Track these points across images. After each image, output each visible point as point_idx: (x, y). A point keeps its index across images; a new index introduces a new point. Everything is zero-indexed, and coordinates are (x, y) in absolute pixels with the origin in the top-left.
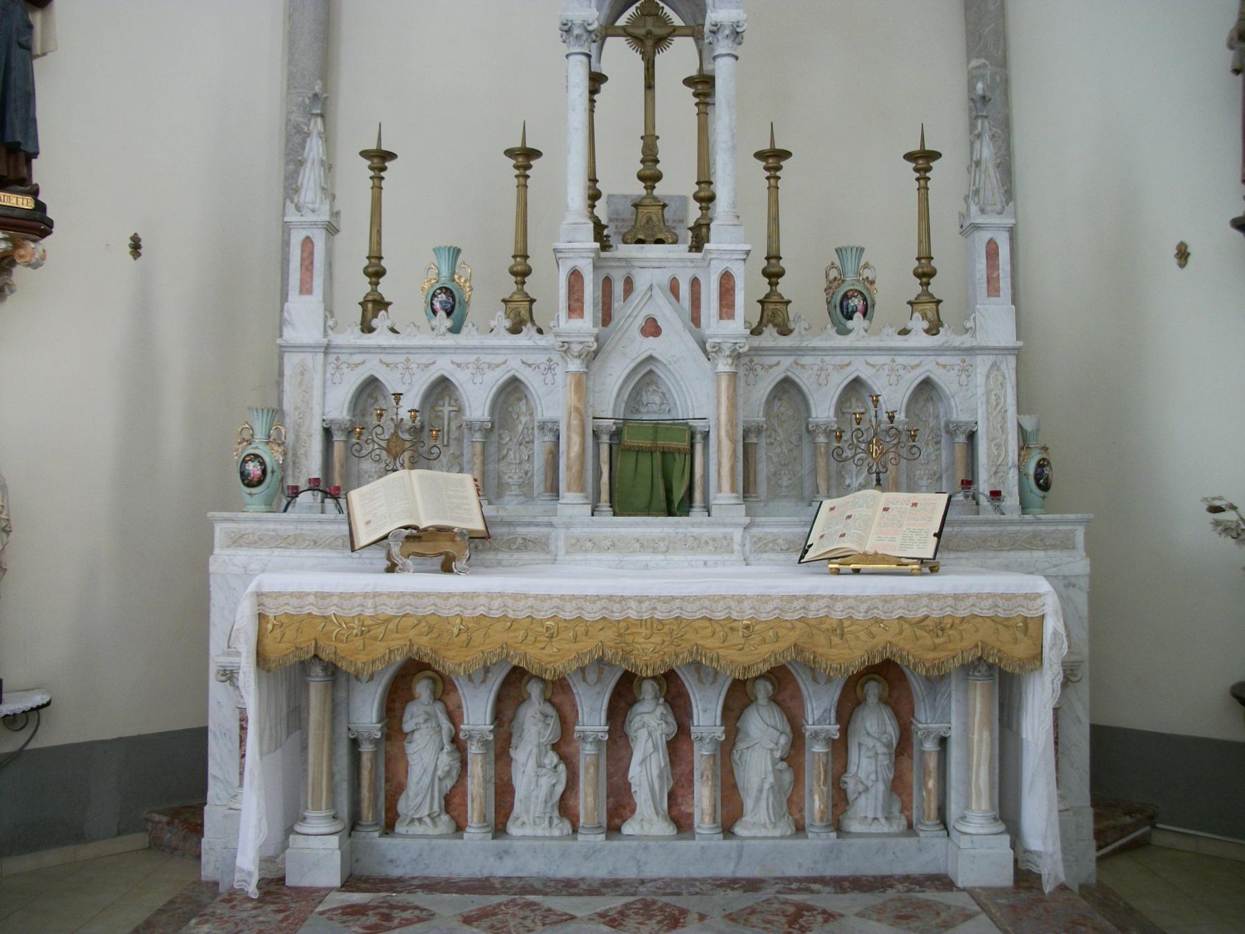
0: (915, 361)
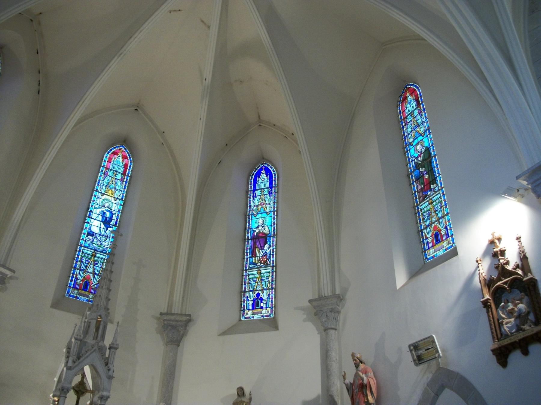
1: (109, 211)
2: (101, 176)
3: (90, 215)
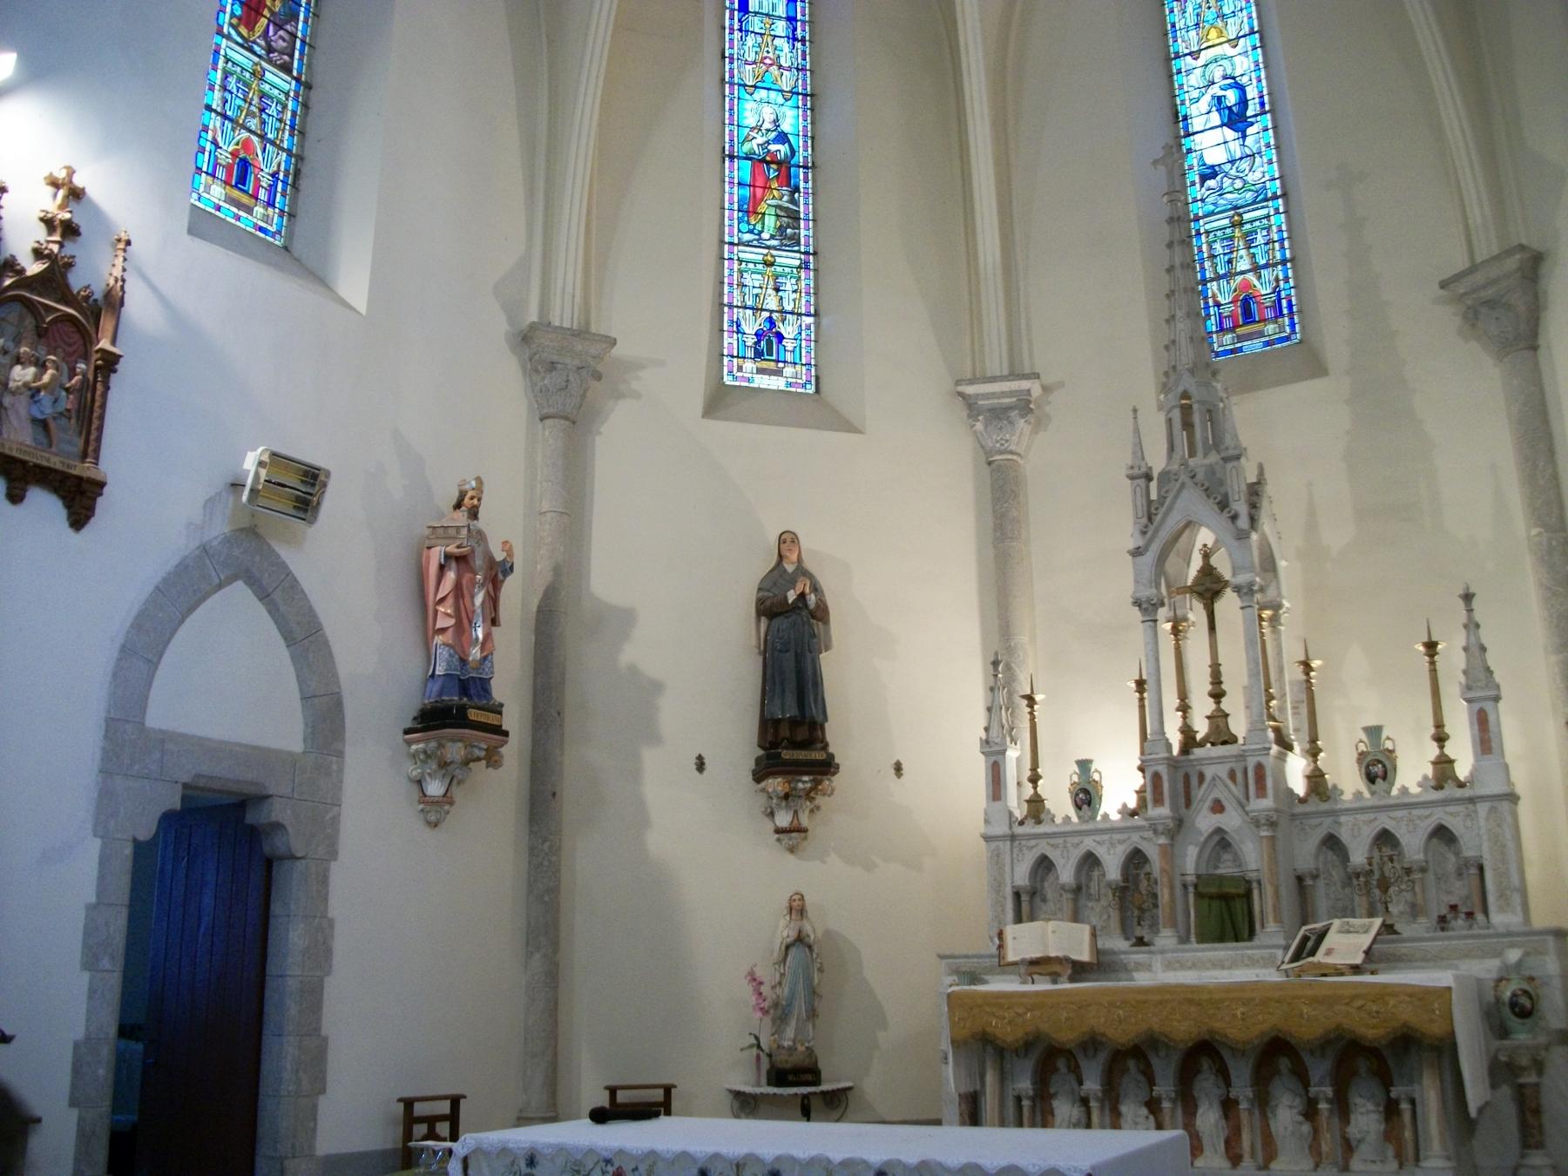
0: (1428, 812)
1: (1230, 86)
2: (1172, 11)
3: (1186, 128)
